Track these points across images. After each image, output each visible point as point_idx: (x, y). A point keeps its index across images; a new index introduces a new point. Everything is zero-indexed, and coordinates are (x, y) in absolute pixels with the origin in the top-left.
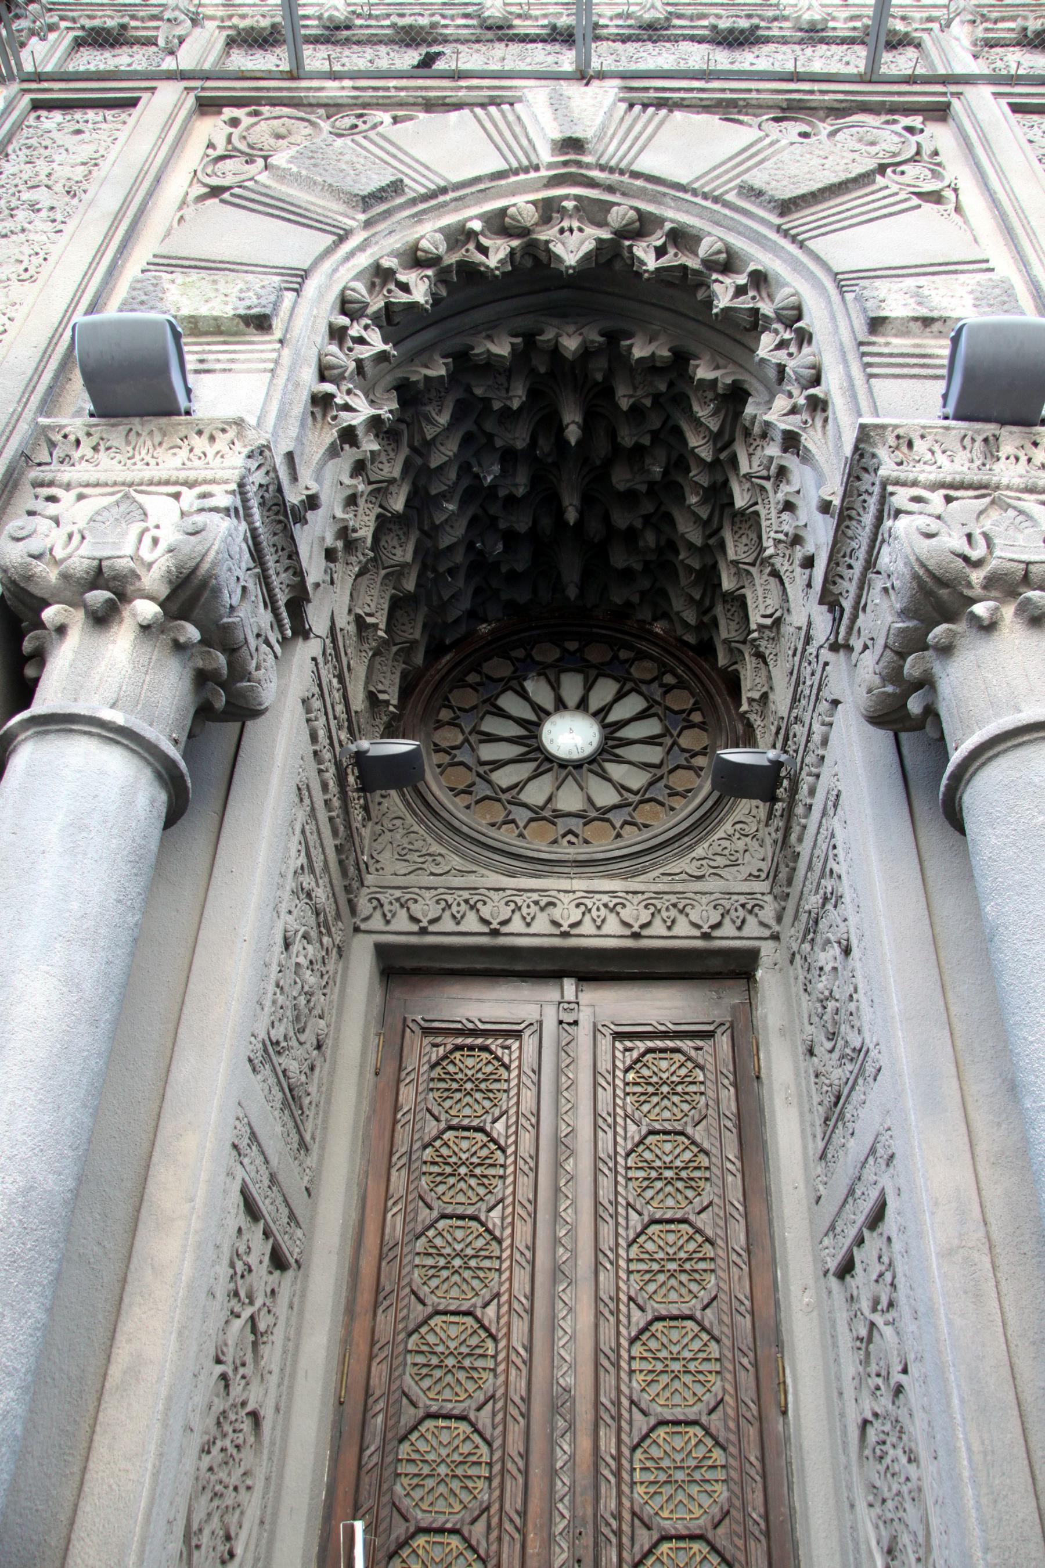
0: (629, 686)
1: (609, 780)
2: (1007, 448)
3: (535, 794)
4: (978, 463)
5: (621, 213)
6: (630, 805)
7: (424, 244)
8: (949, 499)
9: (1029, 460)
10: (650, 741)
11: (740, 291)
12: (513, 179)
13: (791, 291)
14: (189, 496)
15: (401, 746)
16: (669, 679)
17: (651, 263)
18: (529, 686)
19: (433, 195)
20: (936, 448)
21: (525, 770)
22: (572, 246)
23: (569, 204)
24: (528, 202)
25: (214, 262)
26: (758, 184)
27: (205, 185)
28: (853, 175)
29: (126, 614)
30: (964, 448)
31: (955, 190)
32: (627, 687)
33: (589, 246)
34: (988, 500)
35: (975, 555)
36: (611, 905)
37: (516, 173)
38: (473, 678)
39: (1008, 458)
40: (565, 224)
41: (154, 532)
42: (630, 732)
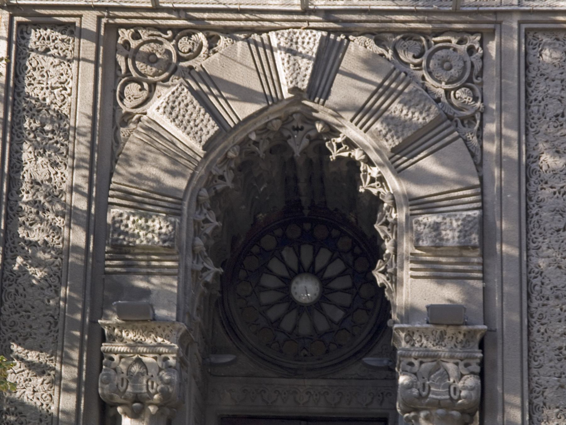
0: (335, 255)
1: (324, 315)
3: (287, 324)
4: (437, 341)
6: (333, 331)
7: (231, 154)
8: (421, 363)
9: (457, 338)
10: (344, 290)
15: (228, 359)
16: (357, 250)
17: (335, 154)
18: (284, 253)
20: (422, 335)
21: (282, 308)
30: (433, 334)
31: (482, 114)
32: (335, 255)
34: (434, 363)
36: (322, 393)
38: (255, 249)
39: (449, 338)
40: (295, 124)
42: (335, 284)
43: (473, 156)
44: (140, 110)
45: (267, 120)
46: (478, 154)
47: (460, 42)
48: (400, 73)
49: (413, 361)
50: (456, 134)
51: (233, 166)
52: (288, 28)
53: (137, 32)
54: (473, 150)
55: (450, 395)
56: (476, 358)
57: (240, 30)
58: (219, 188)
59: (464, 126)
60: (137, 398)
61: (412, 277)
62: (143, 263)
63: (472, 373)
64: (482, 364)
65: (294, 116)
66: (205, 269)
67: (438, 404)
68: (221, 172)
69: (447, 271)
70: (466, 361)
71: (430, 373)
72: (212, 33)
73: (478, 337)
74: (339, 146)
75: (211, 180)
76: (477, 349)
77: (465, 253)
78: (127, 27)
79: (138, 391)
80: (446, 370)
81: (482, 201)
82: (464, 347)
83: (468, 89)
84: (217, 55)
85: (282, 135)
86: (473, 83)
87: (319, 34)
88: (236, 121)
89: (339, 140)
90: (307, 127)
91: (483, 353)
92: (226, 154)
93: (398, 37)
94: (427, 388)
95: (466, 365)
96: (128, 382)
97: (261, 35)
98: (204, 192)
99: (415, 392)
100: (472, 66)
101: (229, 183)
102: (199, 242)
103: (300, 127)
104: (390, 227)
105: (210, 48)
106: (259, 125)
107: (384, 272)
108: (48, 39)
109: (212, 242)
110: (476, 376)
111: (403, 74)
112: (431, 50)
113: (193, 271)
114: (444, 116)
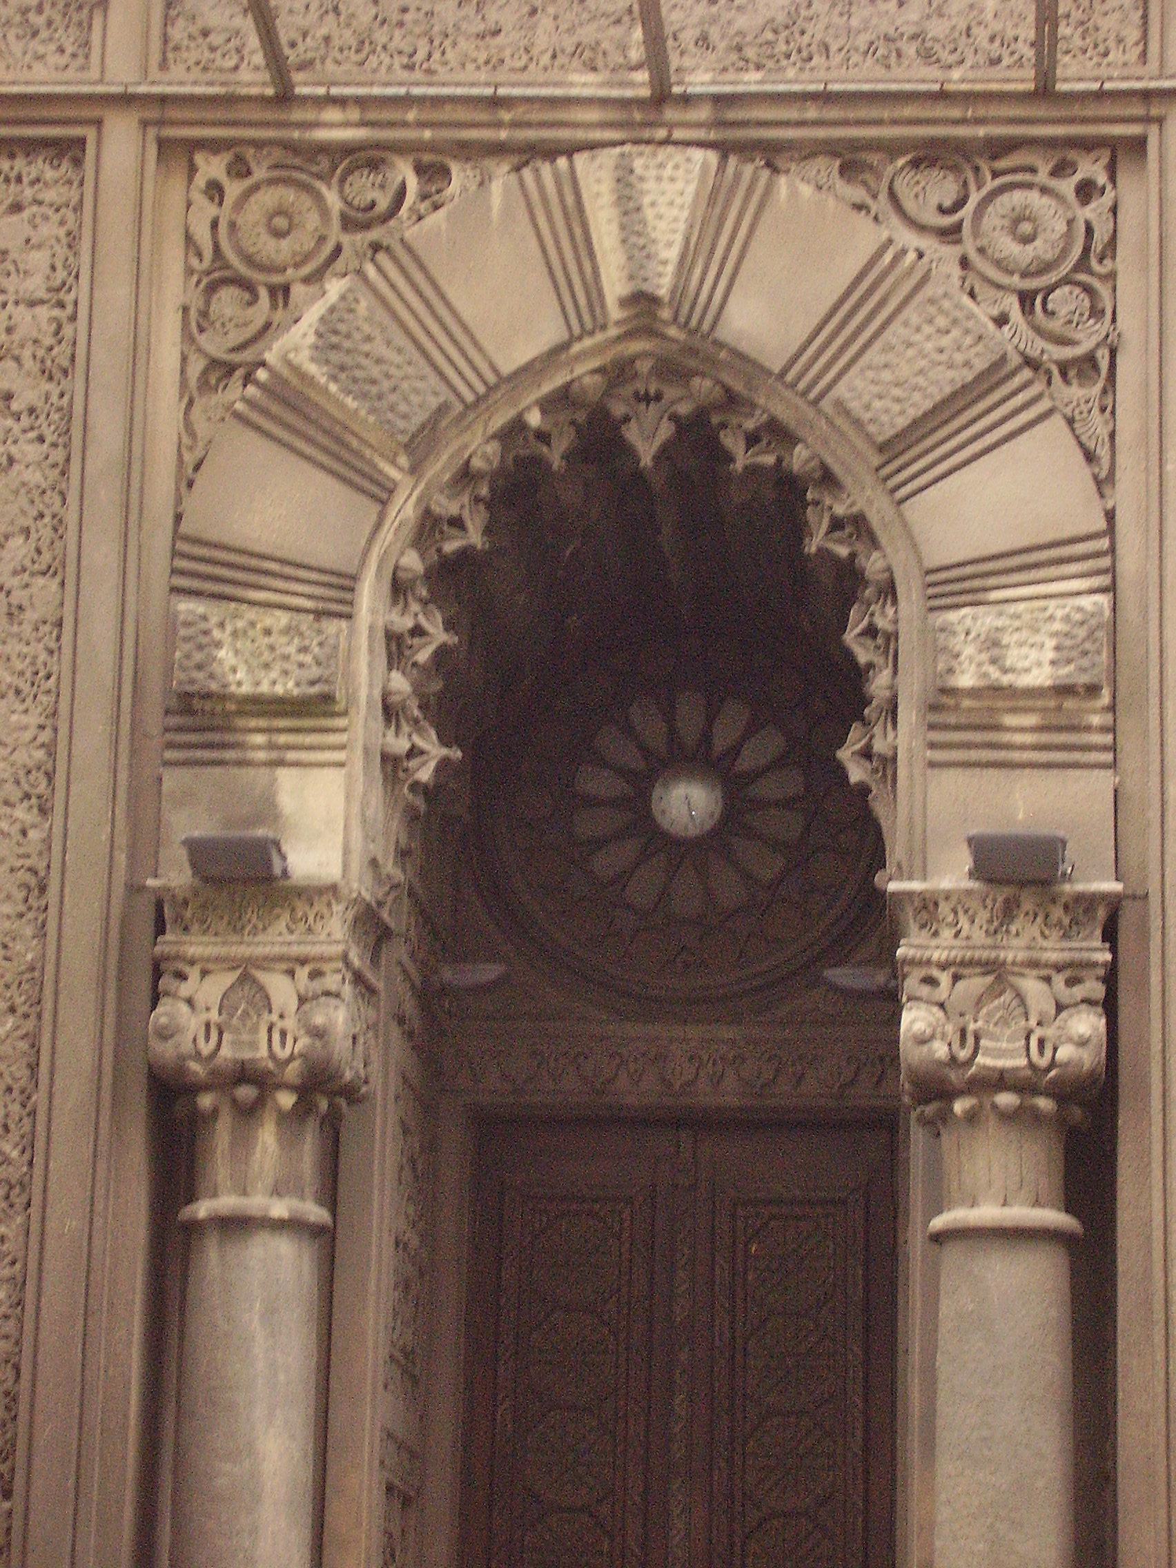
2: (1028, 905)
5: (703, 386)
7: (477, 463)
8: (956, 978)
9: (1047, 916)
11: (837, 524)
12: (576, 348)
13: (880, 564)
14: (303, 973)
19: (479, 399)
22: (647, 439)
23: (644, 366)
24: (595, 371)
25: (252, 554)
26: (855, 406)
27: (206, 355)
28: (969, 376)
29: (269, 1104)
31: (1113, 353)
33: (666, 430)
34: (989, 979)
35: (963, 1054)
37: (580, 338)
40: (640, 386)
41: (280, 1024)
43: (1090, 457)
44: (247, 356)
45: (568, 378)
46: (1103, 452)
47: (1059, 171)
48: (904, 252)
49: (935, 973)
50: (1044, 405)
51: (484, 491)
52: (623, 143)
53: (239, 159)
54: (1091, 445)
55: (1028, 1055)
56: (1094, 965)
57: (498, 150)
58: (450, 547)
59: (1067, 382)
60: (244, 1074)
61: (932, 765)
62: (259, 739)
63: (1088, 1001)
64: (1111, 977)
65: (638, 363)
66: (414, 752)
67: (1000, 1081)
68: (453, 509)
69: (1023, 747)
70: (1068, 973)
71: (979, 1003)
72: (427, 158)
73: (1101, 913)
74: (752, 440)
75: (429, 526)
76: (1097, 943)
77: (1070, 704)
78: (214, 146)
79: (247, 1055)
80: (1020, 997)
81: (1112, 570)
82: (1066, 936)
83: (1077, 290)
84: (442, 213)
85: (607, 414)
86: (1091, 272)
87: (698, 155)
88: (492, 379)
89: (750, 425)
90: (670, 393)
91: (1114, 950)
92: (468, 462)
93: (901, 162)
94: (970, 1040)
95: (1071, 982)
96: (221, 1034)
97: (553, 161)
98: (413, 561)
99: (940, 1050)
100: (1089, 230)
101: (475, 537)
102: (400, 683)
103: (652, 391)
104: (880, 641)
105: (424, 197)
106: (547, 388)
107: (867, 753)
108: (19, 179)
109: (436, 686)
110: (1094, 1009)
111: (911, 256)
112: (984, 191)
113: (386, 758)
114: (1015, 360)
